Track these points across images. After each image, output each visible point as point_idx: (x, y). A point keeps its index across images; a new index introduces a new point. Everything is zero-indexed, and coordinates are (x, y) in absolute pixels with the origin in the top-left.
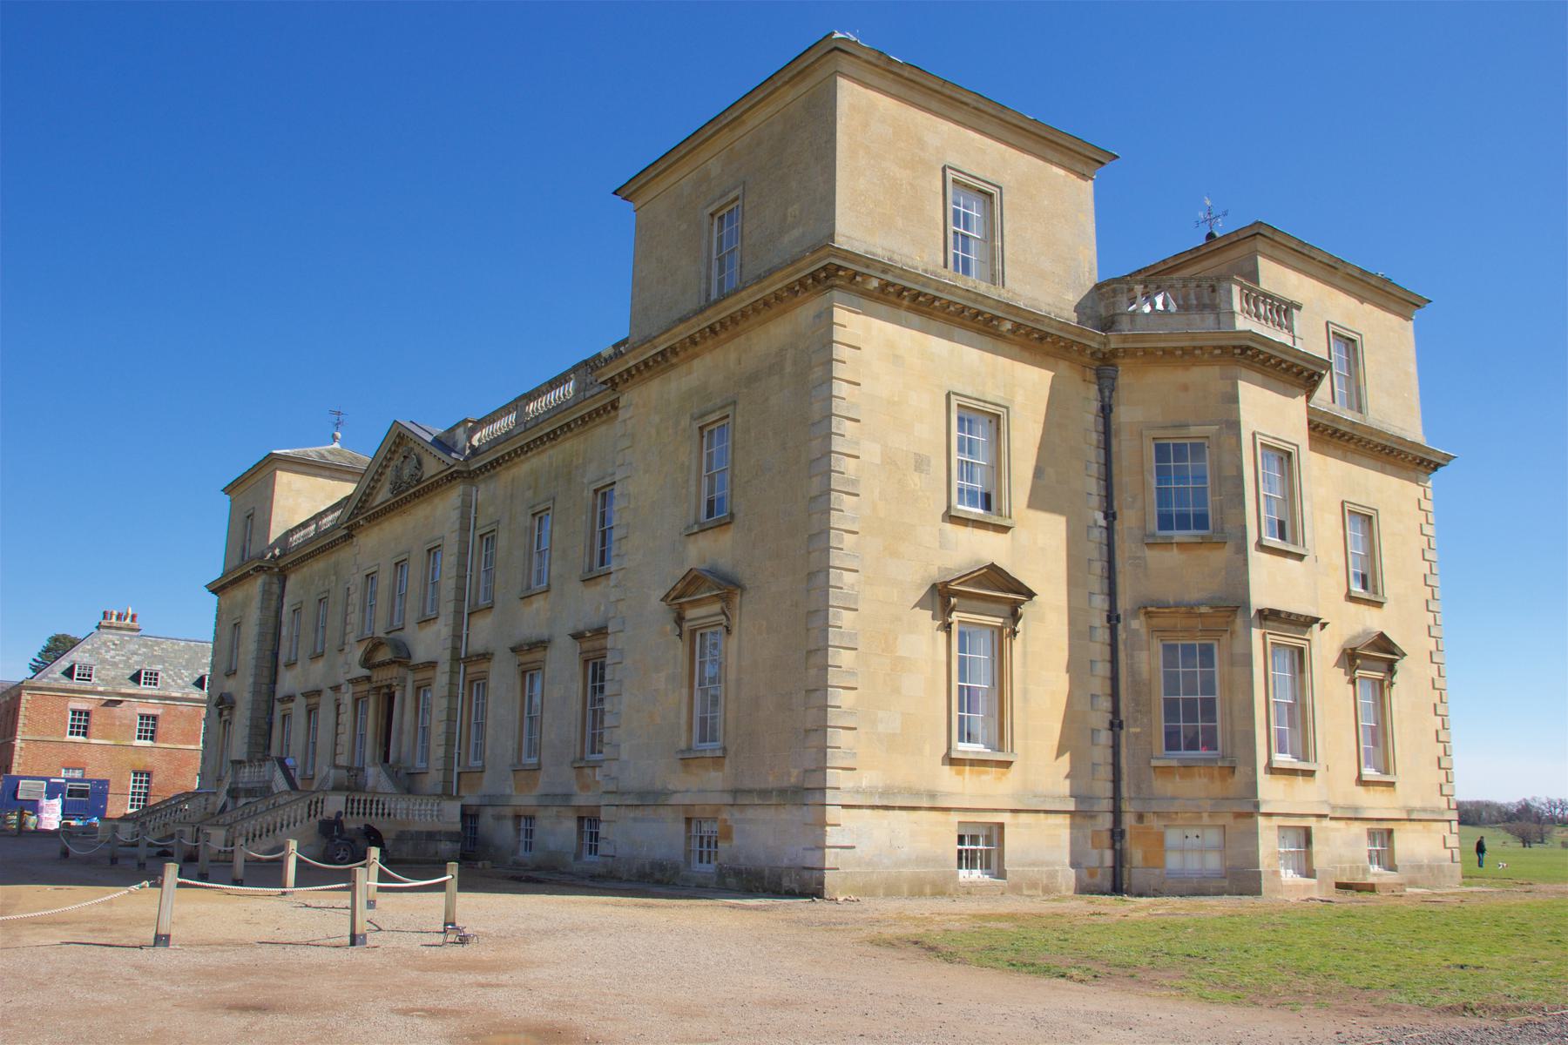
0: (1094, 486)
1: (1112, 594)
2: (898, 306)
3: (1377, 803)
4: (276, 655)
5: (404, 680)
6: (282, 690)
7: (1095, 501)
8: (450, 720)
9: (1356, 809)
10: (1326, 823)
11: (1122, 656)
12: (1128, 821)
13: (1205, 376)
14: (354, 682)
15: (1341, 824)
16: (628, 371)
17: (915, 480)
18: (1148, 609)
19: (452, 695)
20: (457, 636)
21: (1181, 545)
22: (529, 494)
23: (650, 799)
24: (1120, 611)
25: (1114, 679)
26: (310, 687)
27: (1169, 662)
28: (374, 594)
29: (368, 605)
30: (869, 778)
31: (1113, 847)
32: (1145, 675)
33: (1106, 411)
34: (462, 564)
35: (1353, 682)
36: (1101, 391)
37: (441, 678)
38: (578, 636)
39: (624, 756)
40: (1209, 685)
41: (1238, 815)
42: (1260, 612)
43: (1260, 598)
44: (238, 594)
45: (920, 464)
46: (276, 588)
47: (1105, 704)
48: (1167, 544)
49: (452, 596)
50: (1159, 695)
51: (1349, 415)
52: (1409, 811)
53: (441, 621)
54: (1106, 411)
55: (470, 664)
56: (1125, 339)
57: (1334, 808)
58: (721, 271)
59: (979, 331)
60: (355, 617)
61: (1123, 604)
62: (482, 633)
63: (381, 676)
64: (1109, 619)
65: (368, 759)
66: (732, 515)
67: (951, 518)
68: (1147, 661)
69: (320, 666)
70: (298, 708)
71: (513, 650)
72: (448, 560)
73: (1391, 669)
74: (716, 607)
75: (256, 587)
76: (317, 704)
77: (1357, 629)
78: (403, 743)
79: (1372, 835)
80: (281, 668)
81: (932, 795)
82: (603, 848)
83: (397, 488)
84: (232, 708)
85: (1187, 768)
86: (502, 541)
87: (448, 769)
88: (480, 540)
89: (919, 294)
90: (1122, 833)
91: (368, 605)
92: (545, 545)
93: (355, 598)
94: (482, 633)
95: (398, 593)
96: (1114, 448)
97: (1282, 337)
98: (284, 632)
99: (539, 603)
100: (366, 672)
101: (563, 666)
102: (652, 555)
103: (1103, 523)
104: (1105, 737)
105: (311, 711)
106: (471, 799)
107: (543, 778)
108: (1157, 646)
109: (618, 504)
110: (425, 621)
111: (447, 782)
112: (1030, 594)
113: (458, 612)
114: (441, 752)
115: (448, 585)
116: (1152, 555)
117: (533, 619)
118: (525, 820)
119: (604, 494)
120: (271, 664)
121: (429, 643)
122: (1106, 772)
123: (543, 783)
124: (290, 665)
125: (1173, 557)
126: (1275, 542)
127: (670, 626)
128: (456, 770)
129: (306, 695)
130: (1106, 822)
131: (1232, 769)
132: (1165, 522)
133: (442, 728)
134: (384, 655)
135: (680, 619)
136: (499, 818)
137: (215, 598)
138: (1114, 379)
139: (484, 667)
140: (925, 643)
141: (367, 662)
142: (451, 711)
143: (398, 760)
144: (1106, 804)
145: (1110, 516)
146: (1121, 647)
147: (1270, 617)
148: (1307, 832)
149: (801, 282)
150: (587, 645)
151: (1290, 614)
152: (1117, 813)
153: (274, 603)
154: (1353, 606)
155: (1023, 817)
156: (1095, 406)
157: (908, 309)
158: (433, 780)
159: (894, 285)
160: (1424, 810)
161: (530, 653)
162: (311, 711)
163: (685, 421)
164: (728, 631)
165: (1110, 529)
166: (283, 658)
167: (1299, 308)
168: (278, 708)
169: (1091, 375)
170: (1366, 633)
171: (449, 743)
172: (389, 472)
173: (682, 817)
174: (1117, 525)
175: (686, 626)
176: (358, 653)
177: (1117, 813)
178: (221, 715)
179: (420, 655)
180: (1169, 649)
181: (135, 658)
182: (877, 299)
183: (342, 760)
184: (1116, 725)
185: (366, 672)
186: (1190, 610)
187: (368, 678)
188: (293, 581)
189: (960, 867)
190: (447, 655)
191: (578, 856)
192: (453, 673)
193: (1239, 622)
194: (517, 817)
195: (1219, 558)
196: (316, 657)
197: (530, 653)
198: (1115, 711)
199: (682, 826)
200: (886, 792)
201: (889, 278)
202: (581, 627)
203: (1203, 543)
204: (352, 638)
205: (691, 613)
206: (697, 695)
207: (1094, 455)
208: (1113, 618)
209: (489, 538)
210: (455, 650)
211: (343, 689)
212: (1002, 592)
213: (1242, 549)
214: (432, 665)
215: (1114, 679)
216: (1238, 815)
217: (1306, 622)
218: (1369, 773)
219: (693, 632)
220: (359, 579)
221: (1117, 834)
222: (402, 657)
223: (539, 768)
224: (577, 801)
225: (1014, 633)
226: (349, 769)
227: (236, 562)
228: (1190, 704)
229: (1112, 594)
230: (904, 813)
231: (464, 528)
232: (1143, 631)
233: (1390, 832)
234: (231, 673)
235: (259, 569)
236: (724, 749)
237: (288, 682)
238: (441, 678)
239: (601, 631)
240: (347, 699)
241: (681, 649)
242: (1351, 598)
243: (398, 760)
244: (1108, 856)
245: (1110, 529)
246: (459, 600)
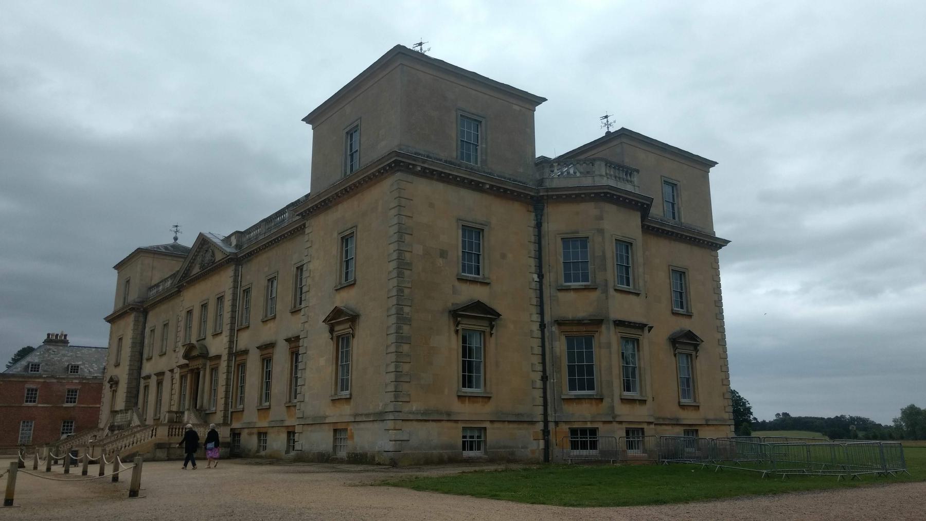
0: (532, 262)
1: (542, 313)
2: (432, 179)
3: (689, 417)
4: (141, 354)
5: (205, 365)
6: (145, 373)
7: (533, 269)
8: (227, 385)
9: (678, 419)
10: (652, 426)
11: (547, 344)
12: (551, 426)
14: (181, 367)
15: (669, 428)
16: (309, 209)
17: (440, 262)
18: (560, 323)
19: (228, 372)
20: (231, 342)
21: (576, 290)
22: (266, 269)
23: (318, 422)
24: (546, 322)
25: (543, 355)
26: (159, 370)
27: (570, 346)
28: (191, 321)
29: (188, 327)
30: (415, 407)
31: (544, 439)
32: (558, 354)
33: (539, 225)
34: (234, 305)
35: (675, 355)
36: (536, 216)
37: (223, 365)
38: (288, 340)
39: (307, 399)
40: (590, 356)
41: (605, 422)
42: (615, 322)
43: (615, 315)
44: (122, 323)
45: (443, 254)
46: (141, 319)
47: (539, 368)
48: (568, 289)
49: (229, 321)
50: (565, 363)
51: (672, 222)
52: (707, 420)
53: (224, 333)
54: (539, 225)
56: (547, 190)
57: (658, 418)
58: (352, 161)
59: (473, 190)
60: (182, 334)
61: (547, 319)
62: (244, 340)
63: (195, 364)
64: (540, 326)
65: (187, 407)
66: (355, 280)
67: (461, 280)
68: (560, 346)
69: (164, 359)
70: (153, 382)
71: (258, 348)
72: (227, 304)
73: (696, 347)
74: (347, 325)
75: (130, 321)
76: (162, 379)
77: (677, 329)
78: (204, 399)
79: (687, 432)
80: (144, 361)
81: (449, 414)
82: (298, 447)
83: (202, 267)
84: (117, 383)
85: (578, 399)
86: (254, 293)
87: (226, 410)
88: (242, 293)
89: (442, 172)
90: (549, 432)
91: (188, 327)
92: (274, 295)
93: (182, 324)
94: (244, 340)
95: (203, 321)
96: (543, 242)
97: (629, 188)
98: (146, 341)
99: (271, 325)
100: (186, 362)
101: (281, 357)
102: (321, 300)
103: (536, 279)
104: (539, 384)
105: (160, 383)
106: (236, 425)
107: (271, 412)
108: (563, 338)
109: (305, 274)
110: (216, 335)
111: (225, 417)
112: (499, 315)
113: (232, 330)
114: (223, 401)
115: (227, 316)
116: (561, 296)
117: (267, 333)
118: (262, 435)
119: (300, 269)
120: (138, 358)
121: (218, 346)
122: (540, 401)
124: (149, 359)
125: (571, 295)
126: (624, 287)
127: (328, 335)
128: (230, 410)
129: (157, 375)
130: (540, 426)
131: (601, 400)
132: (568, 279)
133: (224, 389)
134: (195, 353)
135: (332, 331)
136: (250, 434)
137: (109, 325)
138: (543, 209)
139: (244, 357)
141: (186, 356)
142: (228, 379)
143: (202, 406)
144: (540, 418)
145: (541, 276)
146: (546, 340)
147: (619, 323)
148: (642, 429)
149: (384, 168)
150: (293, 345)
151: (630, 323)
152: (546, 422)
153: (140, 327)
154: (674, 318)
155: (496, 425)
156: (533, 223)
157: (437, 180)
158: (218, 418)
159: (429, 169)
160: (716, 420)
161: (267, 349)
162: (160, 383)
163: (335, 235)
164: (353, 337)
165: (541, 282)
166: (145, 356)
167: (638, 171)
168: (142, 382)
169: (531, 208)
170: (682, 331)
171: (227, 397)
172: (199, 259)
173: (332, 428)
174: (546, 281)
175: (335, 334)
176: (181, 351)
177: (546, 422)
178: (111, 387)
179: (213, 352)
180: (570, 340)
181: (66, 358)
182: (421, 176)
183: (174, 409)
184: (544, 378)
185: (186, 362)
186: (579, 322)
187: (187, 365)
188: (151, 315)
189: (464, 449)
190: (226, 351)
191: (287, 452)
192: (229, 360)
193: (604, 327)
194: (259, 434)
195: (593, 296)
196: (162, 354)
197: (267, 349)
198: (544, 371)
199: (332, 433)
200: (425, 413)
201: (426, 166)
202: (290, 335)
203: (586, 289)
204: (180, 344)
205: (337, 328)
206: (340, 369)
207: (533, 248)
208: (542, 326)
209: (247, 291)
210: (230, 348)
211: (175, 371)
212: (485, 314)
213: (605, 291)
214: (218, 357)
215: (543, 355)
216: (605, 422)
217: (641, 327)
218: (684, 401)
219: (338, 337)
220: (184, 314)
221: (546, 432)
222: (204, 355)
223: (269, 408)
224: (287, 423)
225: (491, 334)
226: (176, 413)
227: (121, 305)
228: (581, 368)
229: (542, 313)
230: (434, 424)
231: (235, 287)
232: (557, 332)
233: (697, 431)
234: (117, 365)
235: (132, 309)
236: (351, 394)
237: (148, 368)
238: (223, 365)
239: (297, 338)
240: (177, 376)
241: (331, 346)
242: (675, 314)
243: (202, 406)
244: (542, 443)
245: (541, 282)
246: (232, 323)
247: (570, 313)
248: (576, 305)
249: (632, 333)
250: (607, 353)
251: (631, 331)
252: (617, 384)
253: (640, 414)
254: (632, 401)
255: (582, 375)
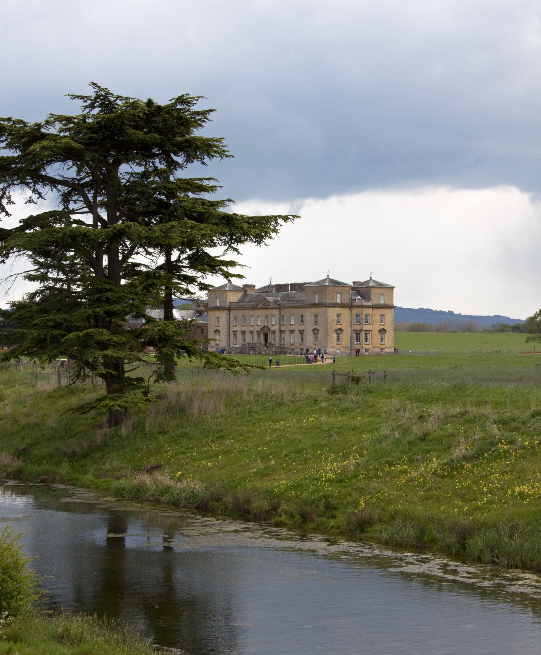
13: (360, 309)
18: (354, 331)
37: (277, 333)
38: (299, 331)
55: (282, 332)
62: (283, 328)
68: (354, 335)
69: (245, 327)
83: (264, 305)
123: (295, 345)
140: (335, 336)
147: (365, 331)
166: (231, 325)
186: (358, 330)
188: (232, 312)
212: (341, 330)
222: (269, 329)
247: (356, 329)
248: (358, 328)
249: (367, 332)
250: (363, 336)
251: (367, 332)
252: (364, 341)
253: (368, 346)
254: (367, 344)
255: (358, 340)
